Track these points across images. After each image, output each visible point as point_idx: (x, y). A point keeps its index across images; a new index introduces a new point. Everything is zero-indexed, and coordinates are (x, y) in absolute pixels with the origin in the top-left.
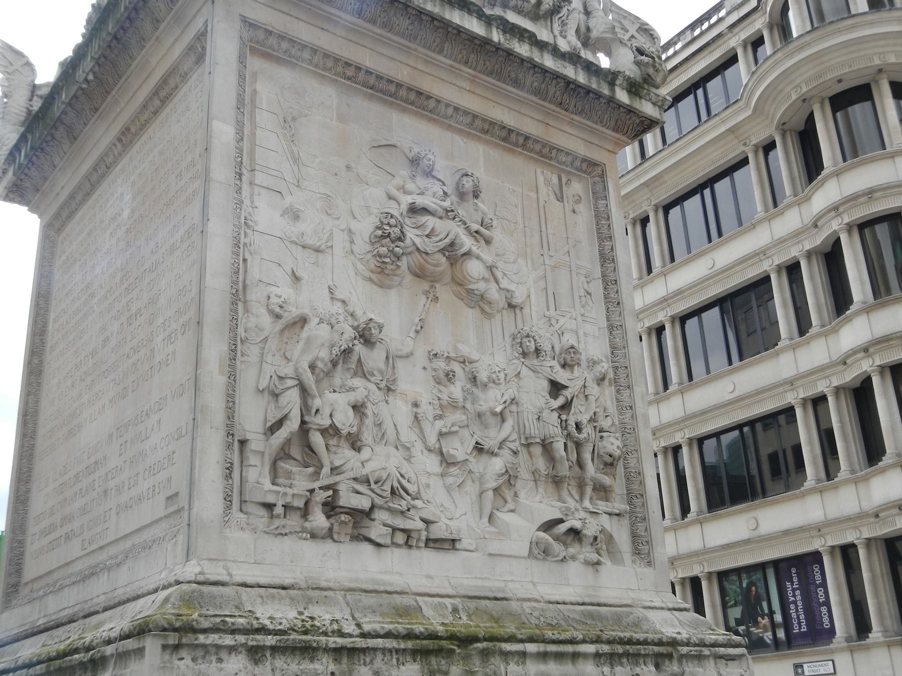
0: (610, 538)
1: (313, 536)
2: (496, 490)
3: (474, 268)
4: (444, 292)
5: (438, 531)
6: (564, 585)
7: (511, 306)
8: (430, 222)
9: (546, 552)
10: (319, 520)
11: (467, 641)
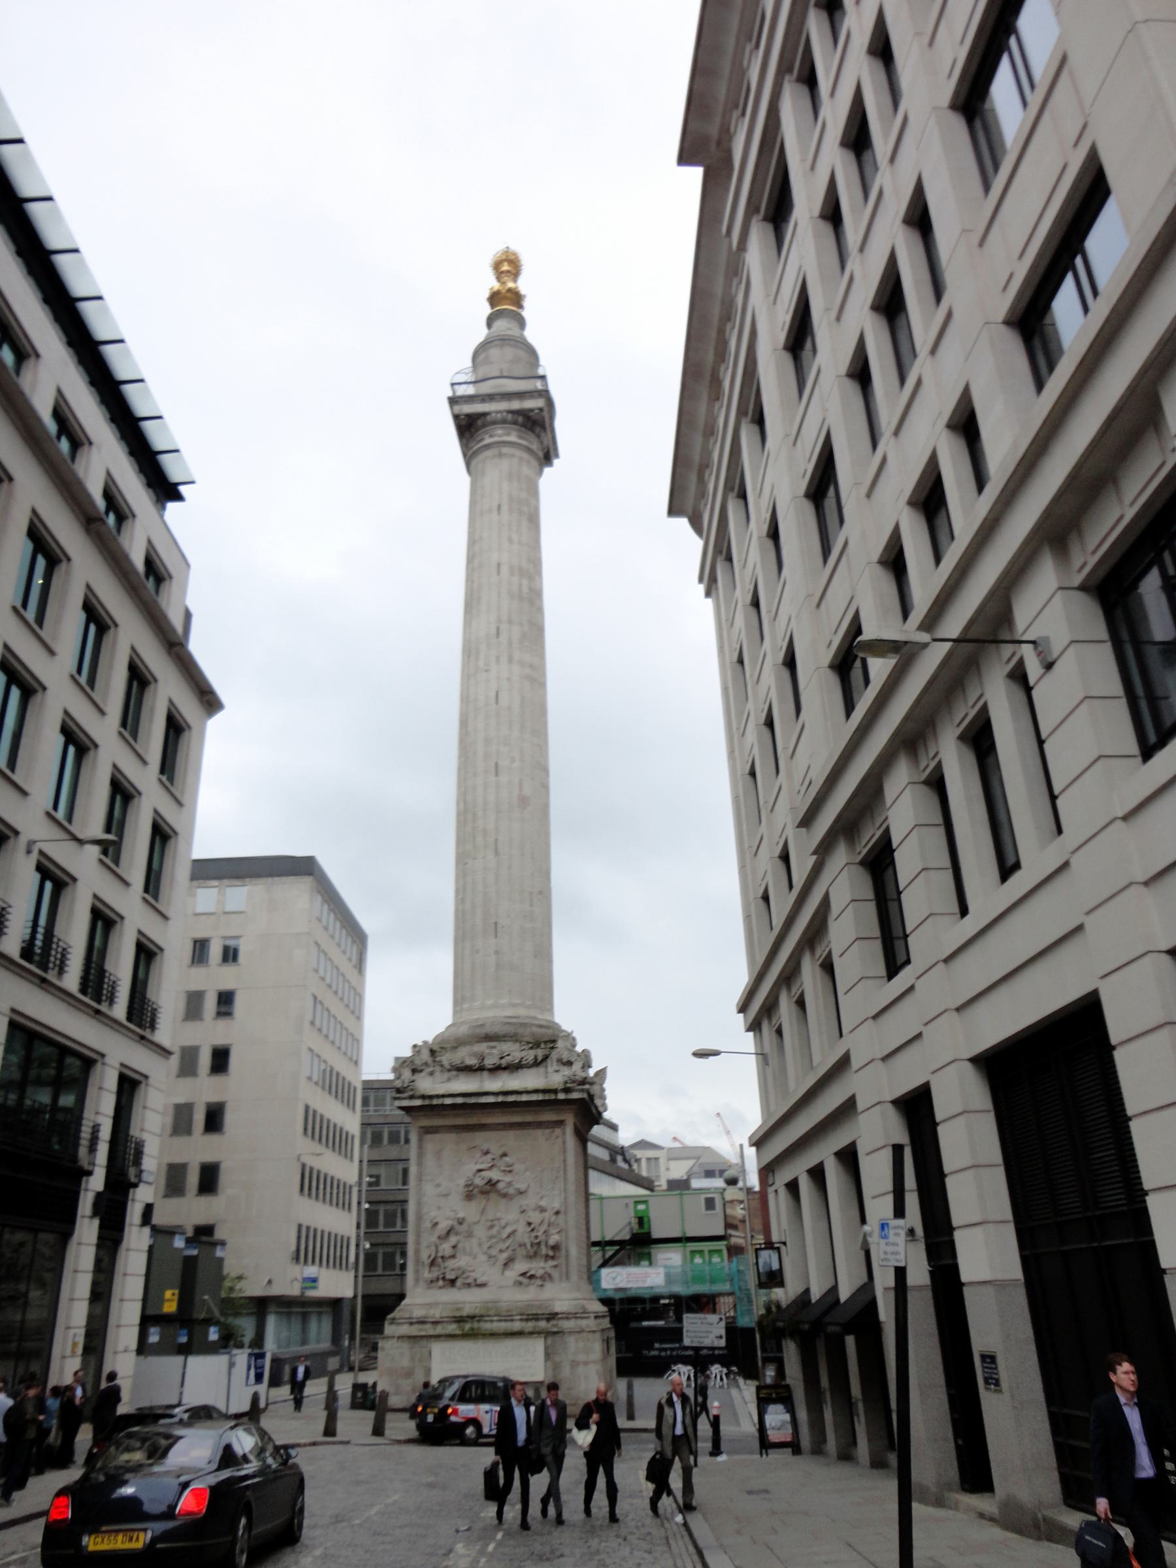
0: (550, 1276)
1: (441, 1288)
2: (505, 1265)
3: (500, 1186)
4: (493, 1196)
5: (479, 1282)
6: (528, 1295)
7: (521, 1193)
8: (483, 1173)
9: (521, 1283)
10: (441, 1283)
11: (472, 1317)
